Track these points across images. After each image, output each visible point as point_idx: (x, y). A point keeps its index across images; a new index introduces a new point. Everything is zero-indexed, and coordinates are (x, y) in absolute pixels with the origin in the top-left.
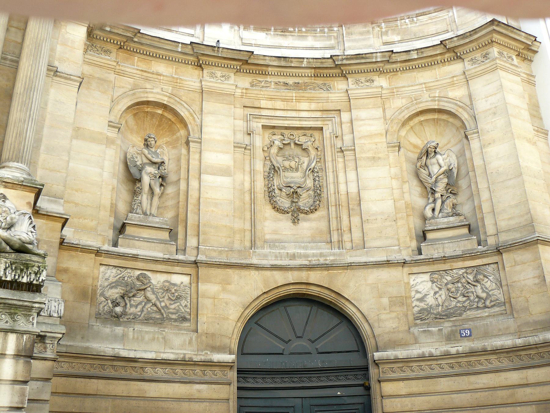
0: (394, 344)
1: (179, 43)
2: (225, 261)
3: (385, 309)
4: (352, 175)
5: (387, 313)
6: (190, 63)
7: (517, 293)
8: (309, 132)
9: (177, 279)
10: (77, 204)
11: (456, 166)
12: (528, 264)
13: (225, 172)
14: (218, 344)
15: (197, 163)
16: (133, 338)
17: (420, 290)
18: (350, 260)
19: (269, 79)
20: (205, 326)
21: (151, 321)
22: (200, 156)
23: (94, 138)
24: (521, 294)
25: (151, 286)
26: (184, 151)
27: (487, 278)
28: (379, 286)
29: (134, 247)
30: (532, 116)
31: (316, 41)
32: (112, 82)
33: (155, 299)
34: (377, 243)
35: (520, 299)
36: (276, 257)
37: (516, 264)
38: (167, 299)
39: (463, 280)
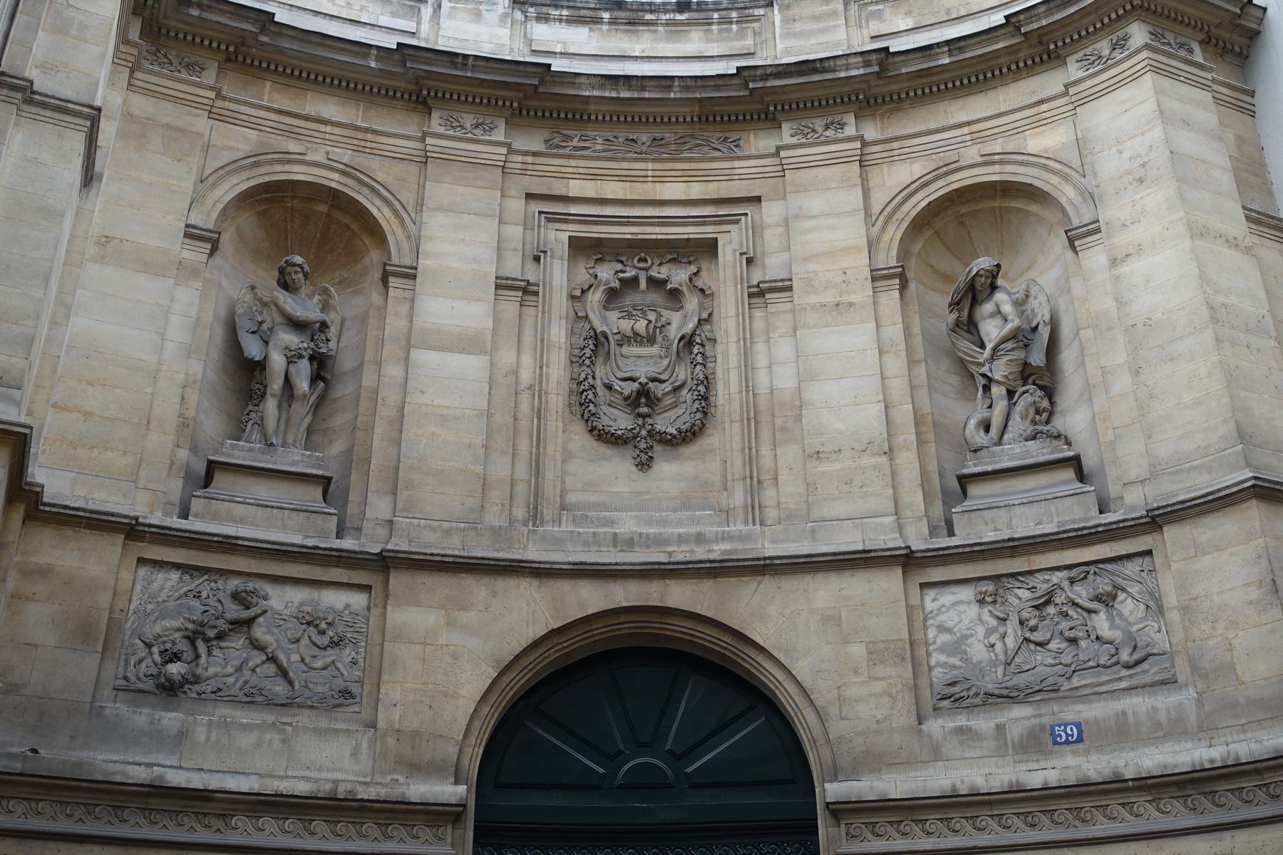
1: (370, 46)
2: (457, 553)
3: (856, 672)
5: (862, 683)
6: (398, 95)
7: (1204, 627)
9: (334, 599)
10: (88, 415)
11: (1047, 318)
12: (1230, 551)
13: (466, 344)
14: (427, 757)
15: (403, 323)
16: (208, 739)
17: (950, 624)
20: (396, 714)
21: (259, 699)
22: (412, 308)
23: (146, 264)
24: (1214, 628)
25: (268, 614)
26: (376, 298)
27: (1124, 590)
28: (844, 614)
29: (231, 519)
30: (1241, 184)
31: (708, 41)
32: (202, 135)
33: (275, 645)
34: (840, 509)
35: (1211, 643)
38: (306, 647)
39: (1060, 598)
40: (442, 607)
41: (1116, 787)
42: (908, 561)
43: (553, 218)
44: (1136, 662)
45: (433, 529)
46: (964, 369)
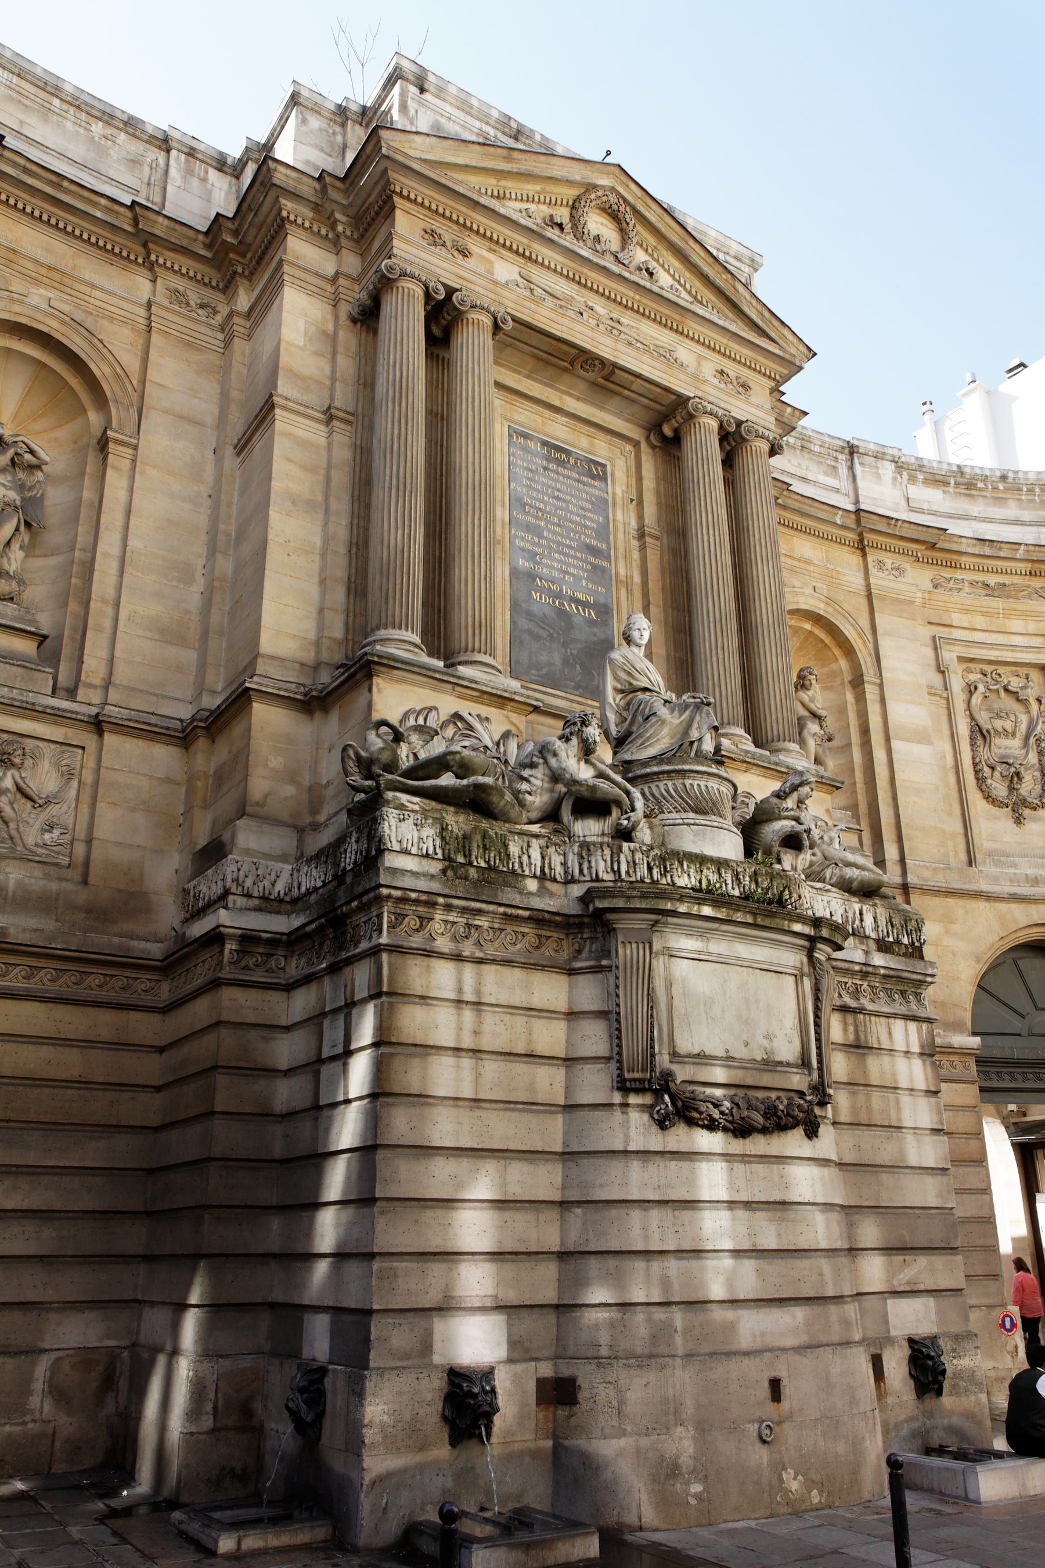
8: (1023, 671)
13: (922, 737)
14: (951, 1019)
19: (959, 575)
36: (1011, 881)
40: (940, 921)
45: (927, 868)
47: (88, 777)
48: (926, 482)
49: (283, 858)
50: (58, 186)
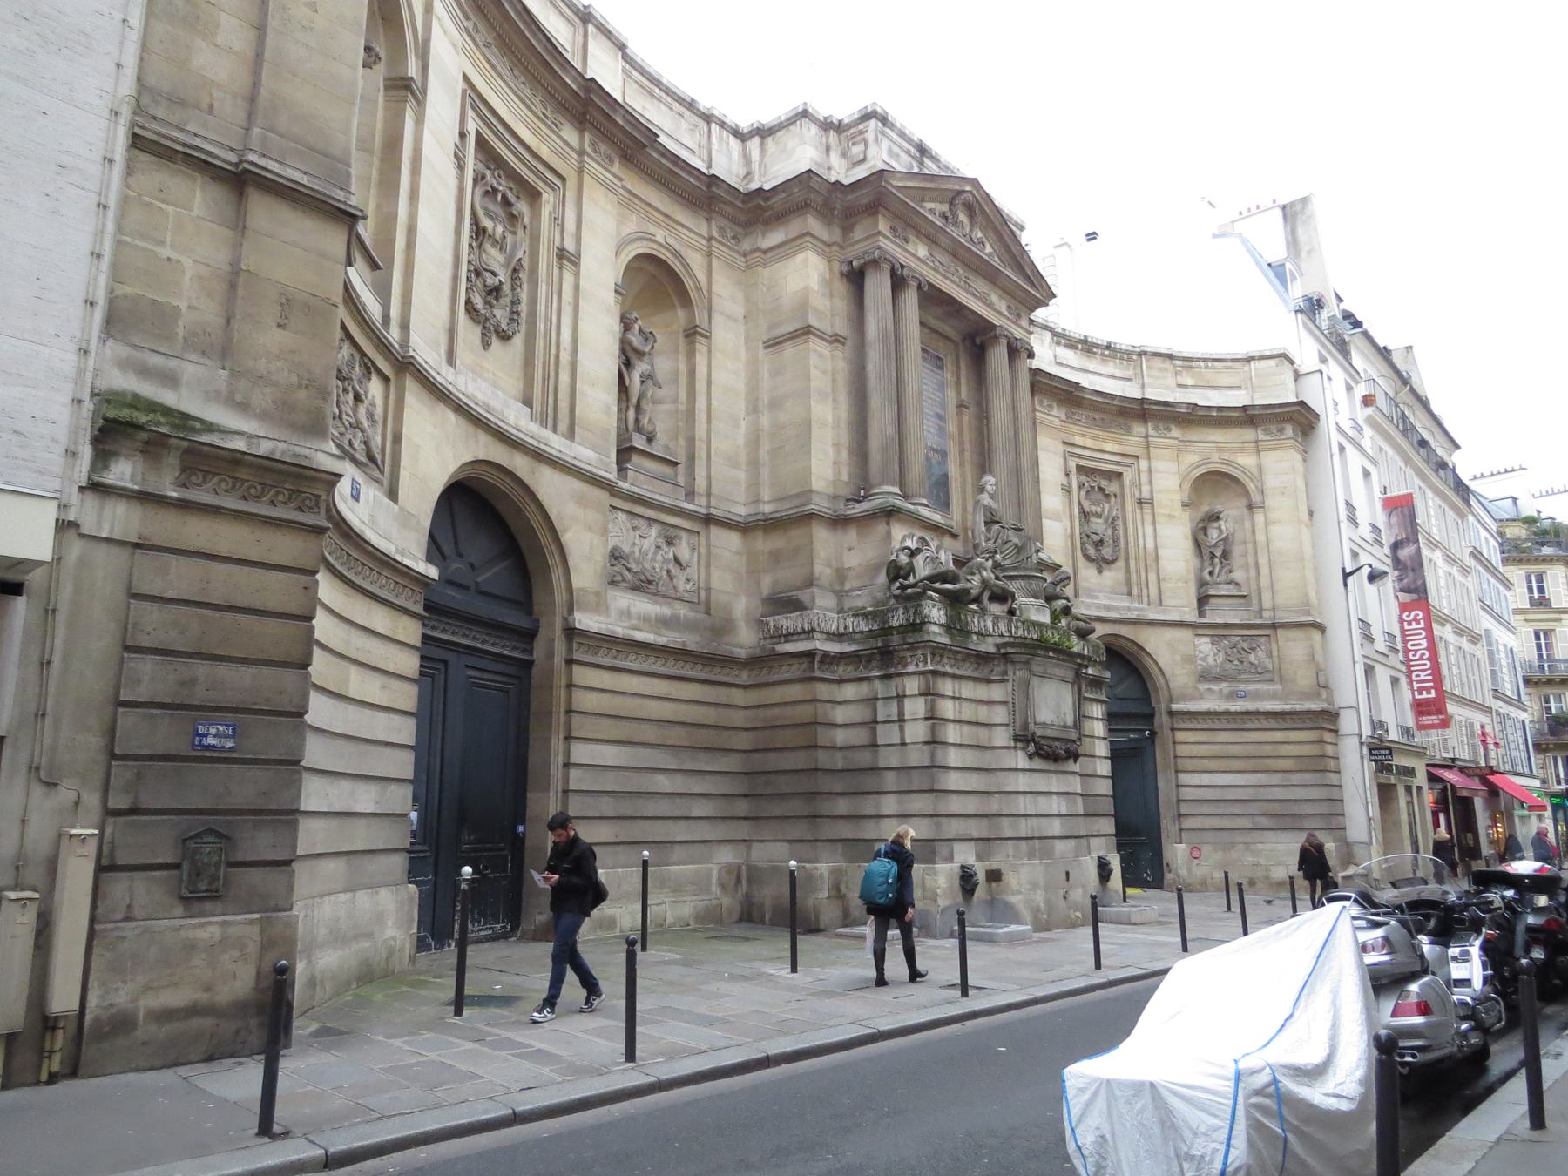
0: (1184, 698)
4: (1149, 530)
18: (1152, 616)
37: (1288, 640)
41: (1257, 713)
42: (1193, 626)
43: (1073, 455)
44: (1259, 672)
46: (1198, 546)
47: (703, 550)
48: (1066, 346)
49: (831, 610)
50: (676, 164)
